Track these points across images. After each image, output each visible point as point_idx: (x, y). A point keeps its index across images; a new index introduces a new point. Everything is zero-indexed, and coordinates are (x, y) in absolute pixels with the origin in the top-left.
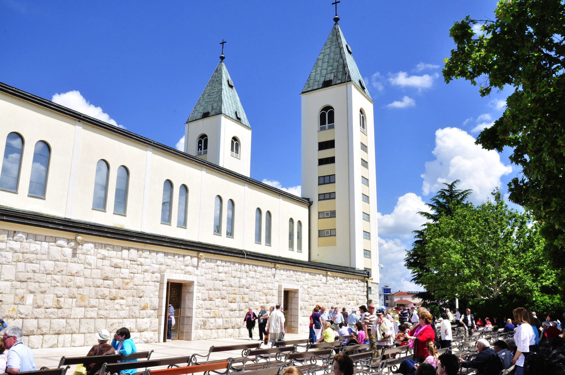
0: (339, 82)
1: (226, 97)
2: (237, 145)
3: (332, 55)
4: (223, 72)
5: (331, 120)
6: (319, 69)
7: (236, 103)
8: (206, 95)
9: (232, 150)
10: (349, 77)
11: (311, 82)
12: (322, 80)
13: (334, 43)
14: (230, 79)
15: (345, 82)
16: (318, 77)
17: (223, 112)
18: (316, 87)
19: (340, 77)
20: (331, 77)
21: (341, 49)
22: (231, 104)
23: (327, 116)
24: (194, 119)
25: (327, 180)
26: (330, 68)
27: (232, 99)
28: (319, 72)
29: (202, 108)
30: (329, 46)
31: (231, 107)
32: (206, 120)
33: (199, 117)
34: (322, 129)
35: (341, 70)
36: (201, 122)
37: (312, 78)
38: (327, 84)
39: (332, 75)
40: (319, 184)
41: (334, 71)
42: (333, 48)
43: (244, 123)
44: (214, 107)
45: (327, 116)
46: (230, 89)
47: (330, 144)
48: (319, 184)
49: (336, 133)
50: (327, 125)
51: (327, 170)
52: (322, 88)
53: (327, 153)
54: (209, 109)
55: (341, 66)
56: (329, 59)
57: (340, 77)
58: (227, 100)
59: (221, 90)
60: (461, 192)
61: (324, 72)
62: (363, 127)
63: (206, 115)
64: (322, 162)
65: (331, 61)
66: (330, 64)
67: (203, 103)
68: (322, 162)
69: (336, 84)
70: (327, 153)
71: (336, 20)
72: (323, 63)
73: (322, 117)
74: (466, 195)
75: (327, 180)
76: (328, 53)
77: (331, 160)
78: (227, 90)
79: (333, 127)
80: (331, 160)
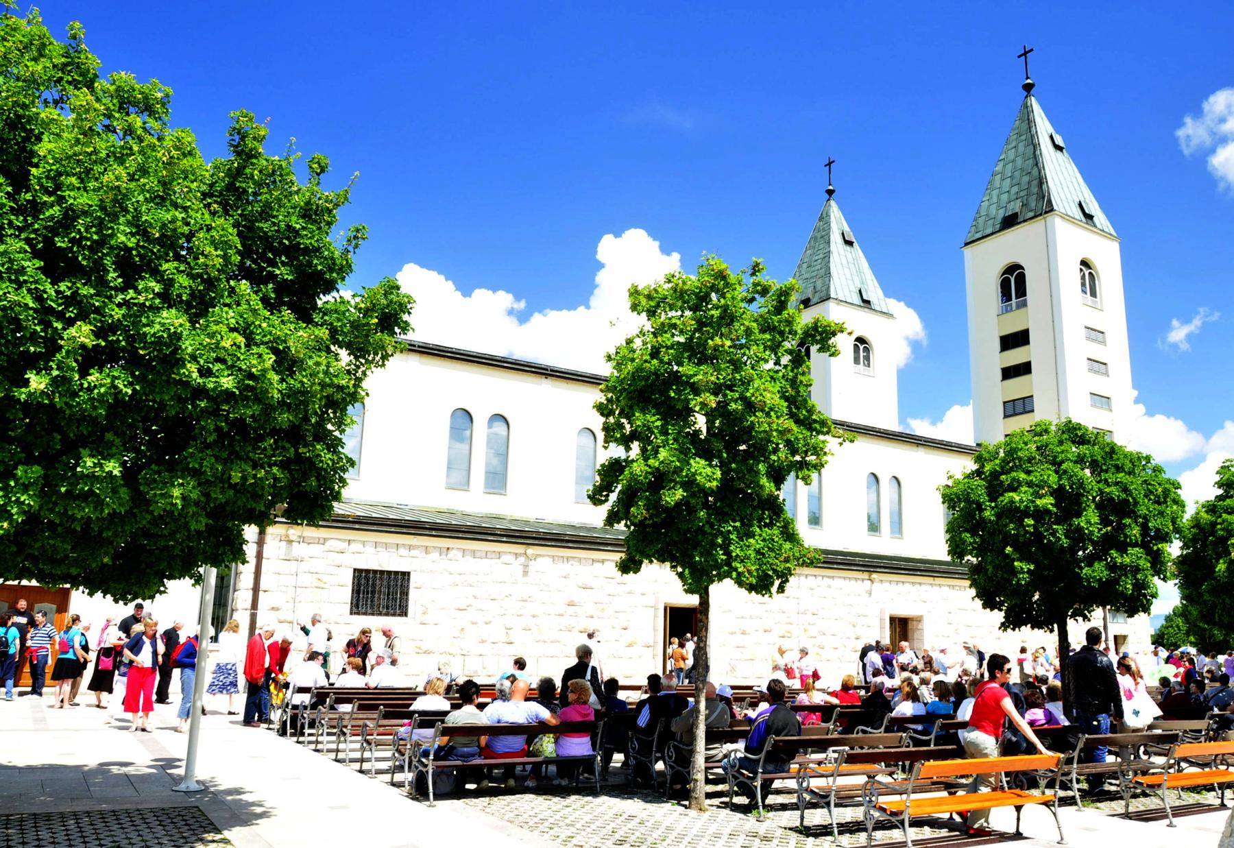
0: (1031, 214)
1: (839, 267)
2: (867, 350)
3: (1019, 161)
4: (833, 219)
5: (1021, 292)
6: (995, 193)
7: (859, 272)
8: (805, 266)
9: (857, 361)
10: (1050, 202)
11: (981, 220)
12: (1001, 214)
13: (1023, 137)
14: (847, 229)
16: (993, 208)
17: (833, 295)
18: (989, 231)
19: (1033, 205)
20: (1016, 207)
21: (1035, 146)
22: (849, 276)
23: (1013, 283)
25: (1019, 407)
26: (1015, 189)
27: (852, 266)
28: (995, 200)
31: (850, 282)
34: (1007, 310)
35: (1035, 190)
37: (983, 213)
38: (1010, 222)
39: (1019, 203)
40: (1006, 416)
41: (1022, 194)
42: (1021, 148)
43: (877, 308)
44: (818, 288)
45: (1013, 283)
46: (848, 248)
48: (1006, 416)
49: (1031, 317)
50: (1014, 300)
51: (1017, 387)
52: (1000, 231)
53: (1016, 356)
55: (1035, 182)
56: (1014, 170)
57: (1033, 205)
58: (840, 271)
59: (827, 255)
61: (1005, 197)
62: (1093, 294)
64: (1009, 373)
65: (1017, 174)
66: (1015, 181)
68: (1009, 373)
69: (1025, 221)
70: (1016, 356)
71: (1028, 88)
72: (1003, 180)
73: (1005, 285)
75: (1019, 407)
76: (1012, 157)
78: (842, 252)
79: (1024, 304)
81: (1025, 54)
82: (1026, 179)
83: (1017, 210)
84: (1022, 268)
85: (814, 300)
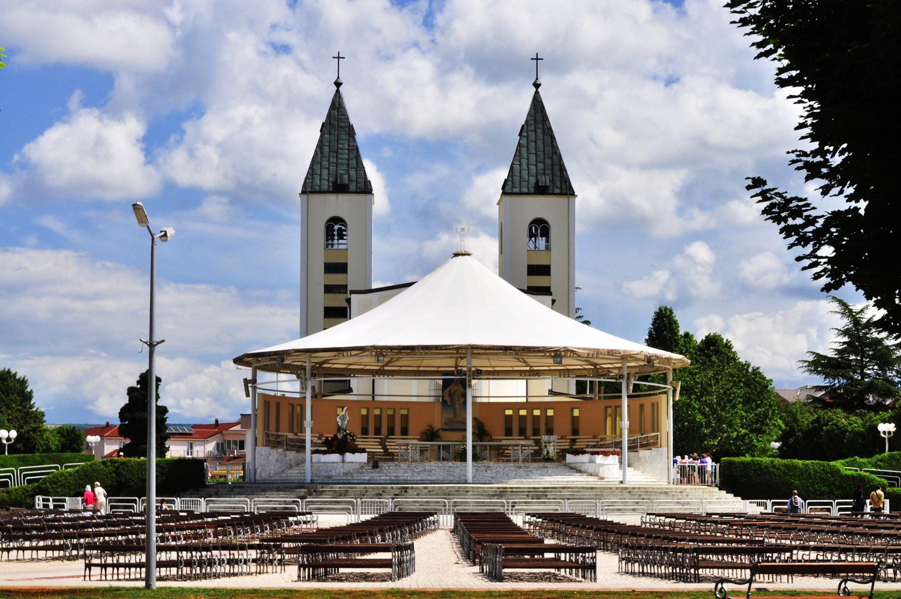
3: (540, 145)
6: (524, 161)
8: (326, 149)
15: (566, 194)
16: (525, 174)
18: (525, 190)
19: (558, 184)
20: (545, 180)
24: (317, 188)
26: (541, 166)
29: (325, 172)
30: (532, 128)
32: (343, 198)
33: (325, 188)
35: (558, 174)
36: (332, 198)
38: (541, 190)
42: (539, 132)
47: (544, 270)
55: (557, 168)
63: (339, 188)
65: (540, 154)
67: (326, 164)
82: (548, 161)
83: (548, 184)
84: (546, 222)
85: (352, 187)
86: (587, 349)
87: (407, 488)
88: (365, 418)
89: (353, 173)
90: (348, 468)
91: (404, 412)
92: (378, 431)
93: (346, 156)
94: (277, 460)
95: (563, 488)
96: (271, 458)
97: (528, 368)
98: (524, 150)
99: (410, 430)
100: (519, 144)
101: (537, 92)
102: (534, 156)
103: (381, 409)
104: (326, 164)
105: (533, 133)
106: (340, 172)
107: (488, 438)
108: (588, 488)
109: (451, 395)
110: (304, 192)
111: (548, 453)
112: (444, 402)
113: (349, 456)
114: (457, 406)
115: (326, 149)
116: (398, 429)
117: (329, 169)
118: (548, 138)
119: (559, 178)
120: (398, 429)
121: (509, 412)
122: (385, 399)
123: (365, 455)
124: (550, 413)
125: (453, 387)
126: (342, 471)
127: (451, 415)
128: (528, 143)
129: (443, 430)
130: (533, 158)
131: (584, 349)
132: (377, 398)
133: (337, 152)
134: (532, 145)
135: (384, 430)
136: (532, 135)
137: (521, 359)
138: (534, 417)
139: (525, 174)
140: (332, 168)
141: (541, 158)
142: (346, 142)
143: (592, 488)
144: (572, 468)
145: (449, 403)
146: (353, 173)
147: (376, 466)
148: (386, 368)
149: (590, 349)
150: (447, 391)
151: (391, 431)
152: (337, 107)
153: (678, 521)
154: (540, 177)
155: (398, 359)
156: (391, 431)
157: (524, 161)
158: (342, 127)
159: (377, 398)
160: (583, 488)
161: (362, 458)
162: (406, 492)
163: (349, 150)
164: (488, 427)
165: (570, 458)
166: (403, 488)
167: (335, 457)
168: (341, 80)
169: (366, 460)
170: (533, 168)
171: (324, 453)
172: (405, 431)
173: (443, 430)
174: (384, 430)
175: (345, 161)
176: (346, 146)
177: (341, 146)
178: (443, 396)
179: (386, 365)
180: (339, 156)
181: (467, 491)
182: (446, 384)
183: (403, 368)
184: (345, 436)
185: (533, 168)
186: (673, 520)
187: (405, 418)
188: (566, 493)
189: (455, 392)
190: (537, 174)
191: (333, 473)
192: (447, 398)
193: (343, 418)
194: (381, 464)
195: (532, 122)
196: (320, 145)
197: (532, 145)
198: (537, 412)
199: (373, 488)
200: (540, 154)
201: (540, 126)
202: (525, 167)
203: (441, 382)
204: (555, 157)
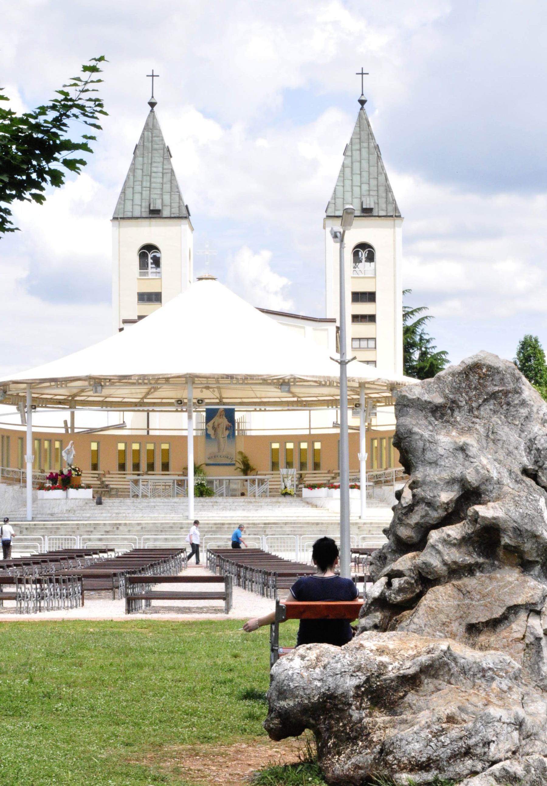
3: (365, 164)
6: (348, 183)
16: (348, 196)
24: (129, 215)
26: (365, 187)
29: (137, 197)
30: (357, 147)
33: (137, 214)
35: (384, 195)
42: (365, 152)
47: (369, 297)
54: (158, 207)
55: (382, 189)
60: (410, 310)
65: (365, 174)
67: (138, 188)
74: (423, 319)
77: (372, 318)
80: (372, 318)
81: (362, 74)
82: (373, 182)
83: (372, 206)
85: (166, 213)
86: (316, 377)
87: (120, 524)
88: (123, 453)
89: (167, 197)
90: (71, 504)
91: (165, 446)
92: (136, 467)
93: (160, 180)
94: (13, 498)
95: (286, 524)
96: (7, 495)
97: (295, 399)
98: (348, 171)
99: (171, 466)
100: (343, 166)
101: (362, 109)
102: (359, 176)
103: (155, 444)
104: (138, 188)
105: (358, 152)
106: (152, 196)
107: (253, 472)
108: (313, 524)
109: (214, 428)
110: (115, 218)
111: (286, 487)
112: (208, 436)
113: (72, 492)
114: (221, 440)
115: (139, 173)
116: (158, 465)
117: (141, 193)
118: (373, 158)
119: (384, 200)
120: (158, 465)
121: (275, 446)
122: (157, 433)
123: (91, 490)
124: (318, 446)
125: (217, 420)
126: (65, 508)
127: (214, 449)
128: (352, 163)
129: (207, 465)
130: (357, 178)
131: (313, 376)
132: (152, 433)
133: (151, 176)
134: (356, 166)
135: (144, 466)
136: (356, 154)
137: (288, 391)
138: (287, 450)
139: (348, 196)
140: (146, 193)
141: (365, 179)
142: (160, 165)
143: (317, 524)
144: (308, 503)
145: (213, 437)
146: (167, 197)
147: (99, 503)
148: (145, 400)
149: (320, 377)
150: (211, 423)
151: (151, 467)
152: (151, 128)
153: (361, 556)
154: (364, 199)
155: (156, 389)
156: (151, 467)
157: (348, 183)
158: (156, 150)
159: (152, 433)
160: (308, 523)
161: (88, 494)
162: (118, 528)
163: (163, 174)
164: (252, 463)
165: (306, 492)
166: (116, 524)
167: (58, 494)
168: (156, 99)
169: (91, 497)
170: (357, 190)
171: (48, 489)
172: (166, 467)
173: (207, 465)
174: (144, 466)
175: (159, 186)
176: (160, 169)
177: (154, 169)
178: (206, 429)
179: (145, 397)
180: (153, 180)
181: (182, 528)
182: (211, 414)
183: (164, 401)
184: (70, 471)
185: (357, 190)
186: (357, 555)
187: (166, 453)
188: (287, 529)
189: (219, 425)
190: (361, 195)
191: (56, 510)
192: (211, 432)
193: (69, 453)
194: (105, 500)
195: (358, 141)
196: (133, 169)
197: (356, 166)
198: (290, 446)
199: (86, 525)
200: (365, 174)
201: (365, 145)
202: (348, 188)
203: (204, 414)
204: (381, 178)
